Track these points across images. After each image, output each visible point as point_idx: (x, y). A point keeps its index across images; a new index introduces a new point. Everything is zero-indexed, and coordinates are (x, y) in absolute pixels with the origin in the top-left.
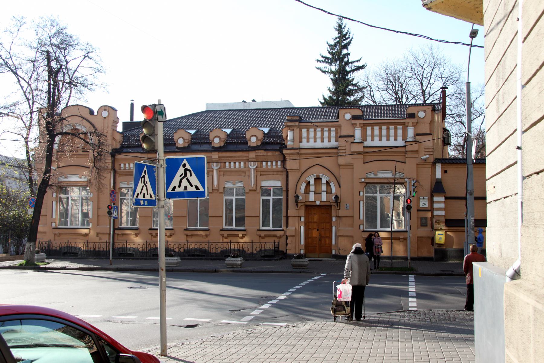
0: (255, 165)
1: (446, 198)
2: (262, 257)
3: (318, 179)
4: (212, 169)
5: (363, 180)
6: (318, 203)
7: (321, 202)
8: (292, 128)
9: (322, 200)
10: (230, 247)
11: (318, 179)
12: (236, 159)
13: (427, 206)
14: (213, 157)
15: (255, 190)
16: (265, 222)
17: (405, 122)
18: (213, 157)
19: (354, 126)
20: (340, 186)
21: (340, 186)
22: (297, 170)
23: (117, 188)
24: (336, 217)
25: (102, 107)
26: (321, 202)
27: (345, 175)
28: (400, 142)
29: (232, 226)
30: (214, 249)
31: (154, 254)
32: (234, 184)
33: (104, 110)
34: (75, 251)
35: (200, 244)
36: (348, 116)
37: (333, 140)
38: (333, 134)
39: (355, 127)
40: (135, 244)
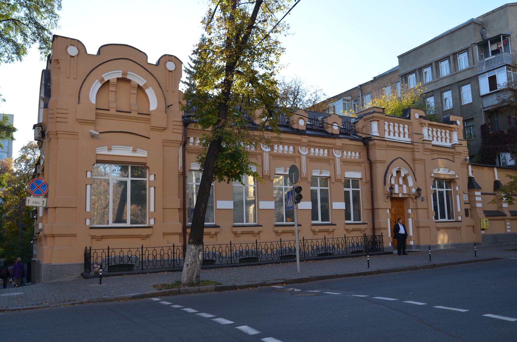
0: (340, 154)
1: (482, 194)
2: (352, 253)
3: (398, 172)
4: (299, 155)
5: (433, 175)
6: (400, 196)
7: (403, 194)
8: (378, 120)
9: (404, 193)
10: (257, 249)
11: (398, 172)
12: (324, 145)
13: (467, 199)
14: (303, 141)
15: (339, 181)
16: (348, 217)
17: (452, 128)
18: (303, 141)
19: (422, 125)
20: (416, 180)
21: (416, 180)
22: (383, 162)
23: (187, 169)
24: (412, 209)
25: (165, 55)
26: (403, 194)
27: (419, 168)
28: (448, 144)
29: (317, 220)
30: (310, 247)
31: (241, 258)
32: (321, 173)
33: (169, 61)
34: (130, 263)
35: (137, 249)
36: (417, 116)
37: (407, 136)
38: (406, 130)
39: (423, 126)
40: (221, 246)
